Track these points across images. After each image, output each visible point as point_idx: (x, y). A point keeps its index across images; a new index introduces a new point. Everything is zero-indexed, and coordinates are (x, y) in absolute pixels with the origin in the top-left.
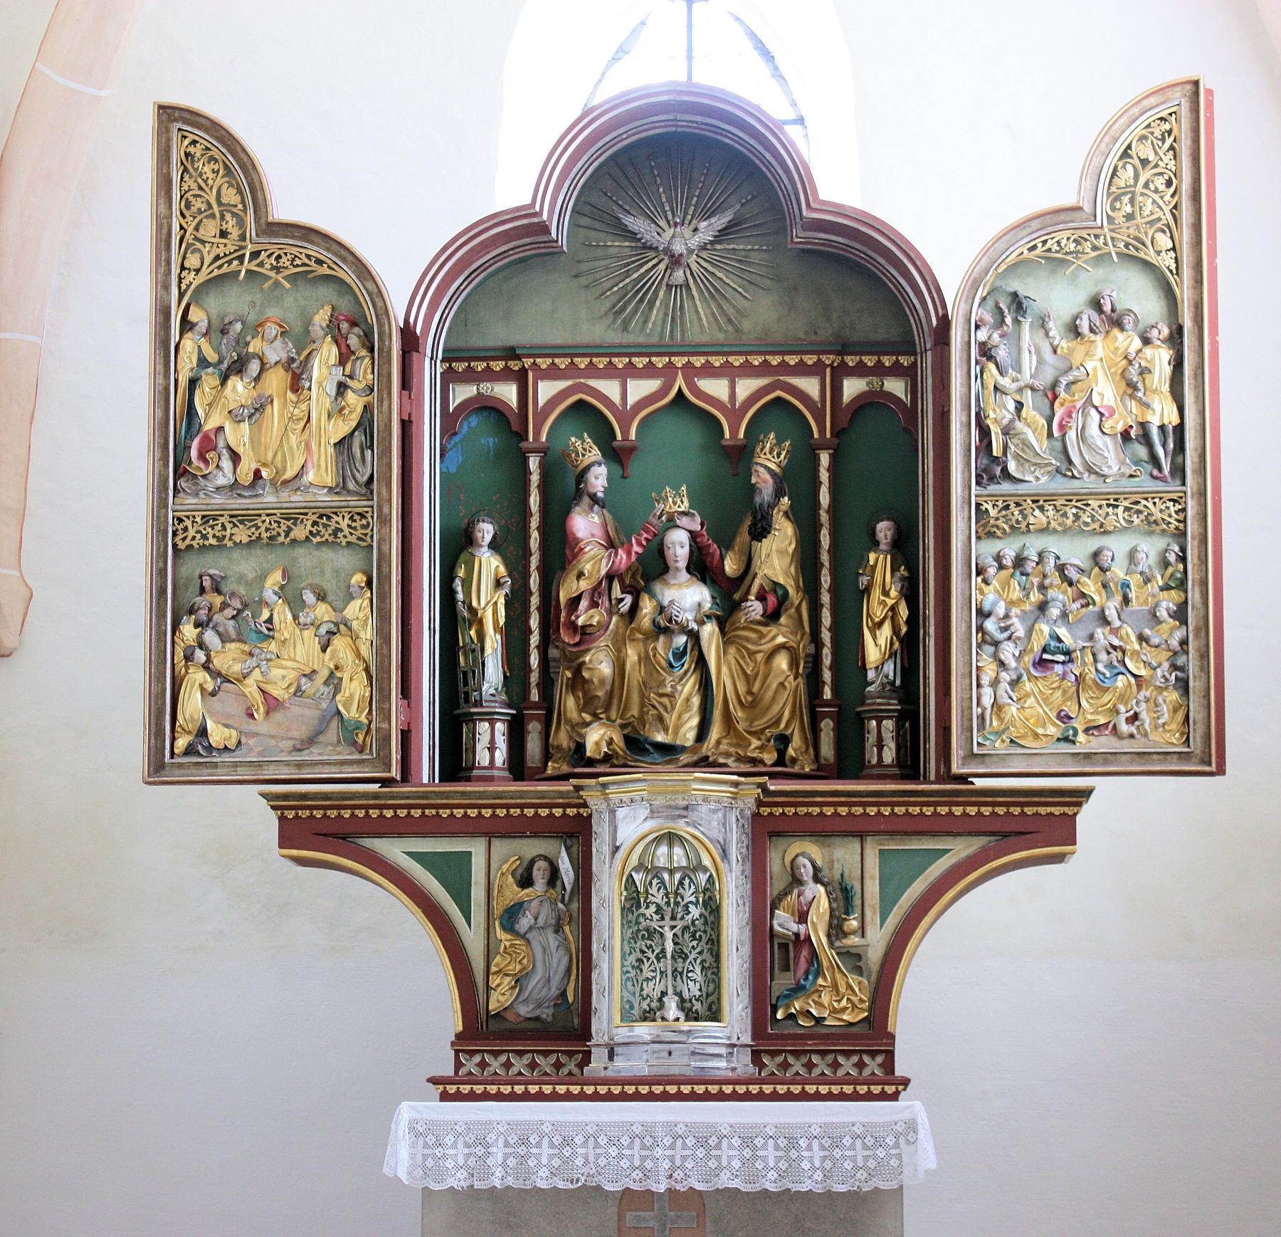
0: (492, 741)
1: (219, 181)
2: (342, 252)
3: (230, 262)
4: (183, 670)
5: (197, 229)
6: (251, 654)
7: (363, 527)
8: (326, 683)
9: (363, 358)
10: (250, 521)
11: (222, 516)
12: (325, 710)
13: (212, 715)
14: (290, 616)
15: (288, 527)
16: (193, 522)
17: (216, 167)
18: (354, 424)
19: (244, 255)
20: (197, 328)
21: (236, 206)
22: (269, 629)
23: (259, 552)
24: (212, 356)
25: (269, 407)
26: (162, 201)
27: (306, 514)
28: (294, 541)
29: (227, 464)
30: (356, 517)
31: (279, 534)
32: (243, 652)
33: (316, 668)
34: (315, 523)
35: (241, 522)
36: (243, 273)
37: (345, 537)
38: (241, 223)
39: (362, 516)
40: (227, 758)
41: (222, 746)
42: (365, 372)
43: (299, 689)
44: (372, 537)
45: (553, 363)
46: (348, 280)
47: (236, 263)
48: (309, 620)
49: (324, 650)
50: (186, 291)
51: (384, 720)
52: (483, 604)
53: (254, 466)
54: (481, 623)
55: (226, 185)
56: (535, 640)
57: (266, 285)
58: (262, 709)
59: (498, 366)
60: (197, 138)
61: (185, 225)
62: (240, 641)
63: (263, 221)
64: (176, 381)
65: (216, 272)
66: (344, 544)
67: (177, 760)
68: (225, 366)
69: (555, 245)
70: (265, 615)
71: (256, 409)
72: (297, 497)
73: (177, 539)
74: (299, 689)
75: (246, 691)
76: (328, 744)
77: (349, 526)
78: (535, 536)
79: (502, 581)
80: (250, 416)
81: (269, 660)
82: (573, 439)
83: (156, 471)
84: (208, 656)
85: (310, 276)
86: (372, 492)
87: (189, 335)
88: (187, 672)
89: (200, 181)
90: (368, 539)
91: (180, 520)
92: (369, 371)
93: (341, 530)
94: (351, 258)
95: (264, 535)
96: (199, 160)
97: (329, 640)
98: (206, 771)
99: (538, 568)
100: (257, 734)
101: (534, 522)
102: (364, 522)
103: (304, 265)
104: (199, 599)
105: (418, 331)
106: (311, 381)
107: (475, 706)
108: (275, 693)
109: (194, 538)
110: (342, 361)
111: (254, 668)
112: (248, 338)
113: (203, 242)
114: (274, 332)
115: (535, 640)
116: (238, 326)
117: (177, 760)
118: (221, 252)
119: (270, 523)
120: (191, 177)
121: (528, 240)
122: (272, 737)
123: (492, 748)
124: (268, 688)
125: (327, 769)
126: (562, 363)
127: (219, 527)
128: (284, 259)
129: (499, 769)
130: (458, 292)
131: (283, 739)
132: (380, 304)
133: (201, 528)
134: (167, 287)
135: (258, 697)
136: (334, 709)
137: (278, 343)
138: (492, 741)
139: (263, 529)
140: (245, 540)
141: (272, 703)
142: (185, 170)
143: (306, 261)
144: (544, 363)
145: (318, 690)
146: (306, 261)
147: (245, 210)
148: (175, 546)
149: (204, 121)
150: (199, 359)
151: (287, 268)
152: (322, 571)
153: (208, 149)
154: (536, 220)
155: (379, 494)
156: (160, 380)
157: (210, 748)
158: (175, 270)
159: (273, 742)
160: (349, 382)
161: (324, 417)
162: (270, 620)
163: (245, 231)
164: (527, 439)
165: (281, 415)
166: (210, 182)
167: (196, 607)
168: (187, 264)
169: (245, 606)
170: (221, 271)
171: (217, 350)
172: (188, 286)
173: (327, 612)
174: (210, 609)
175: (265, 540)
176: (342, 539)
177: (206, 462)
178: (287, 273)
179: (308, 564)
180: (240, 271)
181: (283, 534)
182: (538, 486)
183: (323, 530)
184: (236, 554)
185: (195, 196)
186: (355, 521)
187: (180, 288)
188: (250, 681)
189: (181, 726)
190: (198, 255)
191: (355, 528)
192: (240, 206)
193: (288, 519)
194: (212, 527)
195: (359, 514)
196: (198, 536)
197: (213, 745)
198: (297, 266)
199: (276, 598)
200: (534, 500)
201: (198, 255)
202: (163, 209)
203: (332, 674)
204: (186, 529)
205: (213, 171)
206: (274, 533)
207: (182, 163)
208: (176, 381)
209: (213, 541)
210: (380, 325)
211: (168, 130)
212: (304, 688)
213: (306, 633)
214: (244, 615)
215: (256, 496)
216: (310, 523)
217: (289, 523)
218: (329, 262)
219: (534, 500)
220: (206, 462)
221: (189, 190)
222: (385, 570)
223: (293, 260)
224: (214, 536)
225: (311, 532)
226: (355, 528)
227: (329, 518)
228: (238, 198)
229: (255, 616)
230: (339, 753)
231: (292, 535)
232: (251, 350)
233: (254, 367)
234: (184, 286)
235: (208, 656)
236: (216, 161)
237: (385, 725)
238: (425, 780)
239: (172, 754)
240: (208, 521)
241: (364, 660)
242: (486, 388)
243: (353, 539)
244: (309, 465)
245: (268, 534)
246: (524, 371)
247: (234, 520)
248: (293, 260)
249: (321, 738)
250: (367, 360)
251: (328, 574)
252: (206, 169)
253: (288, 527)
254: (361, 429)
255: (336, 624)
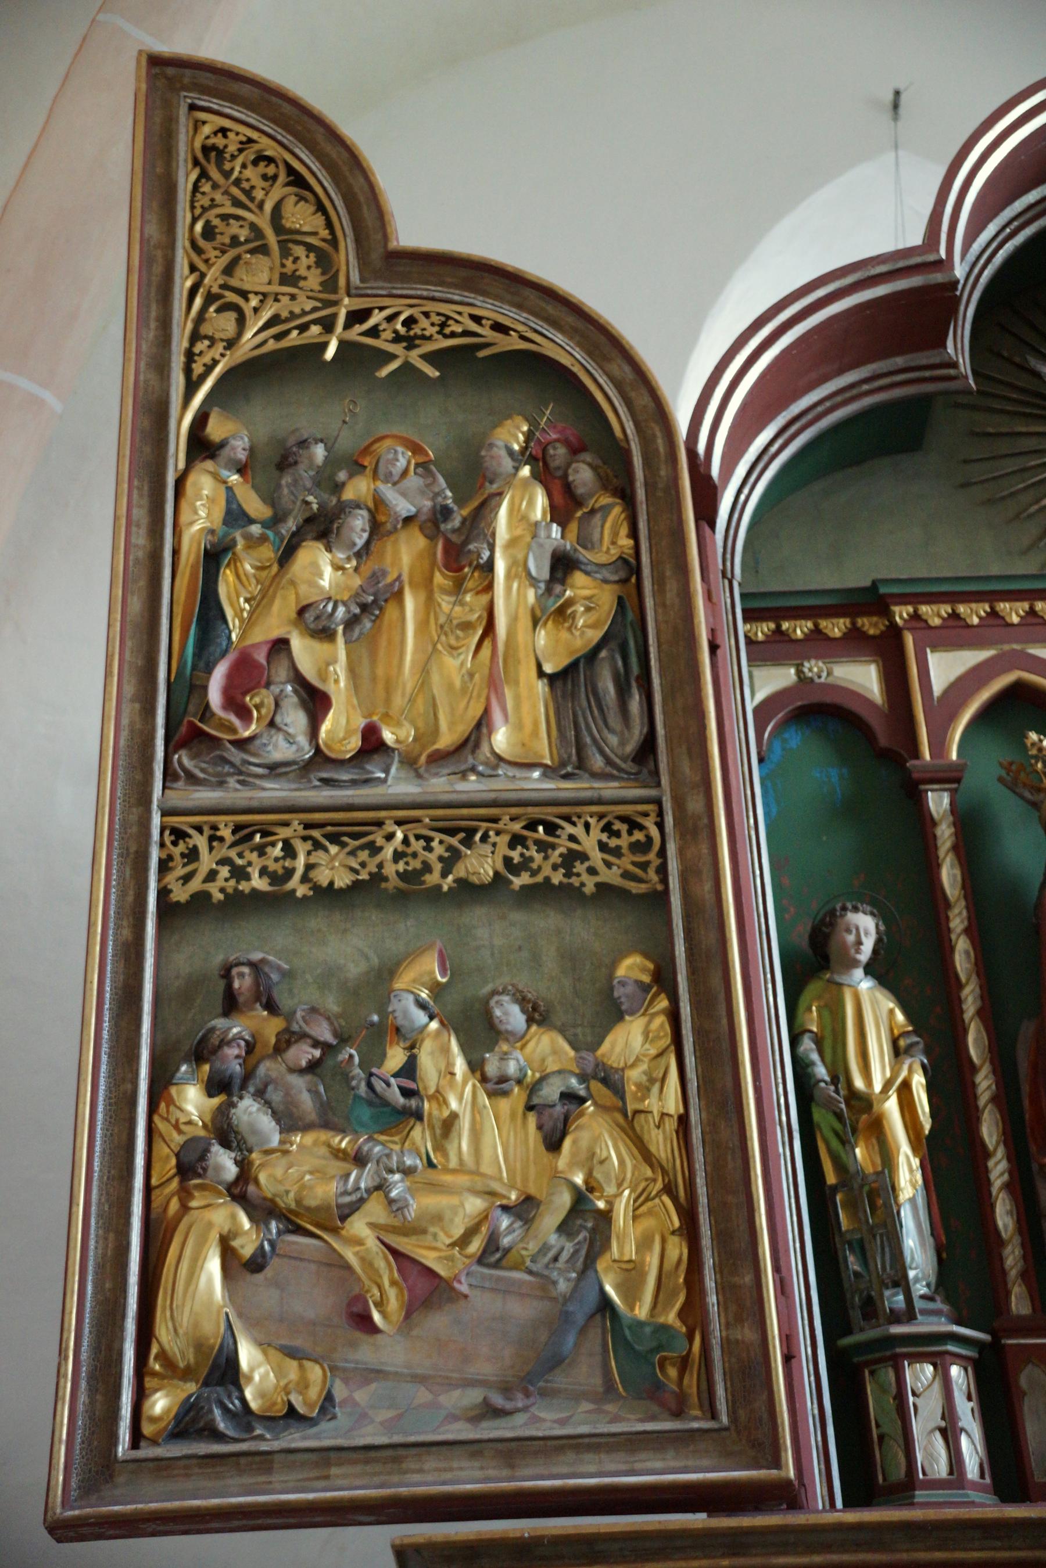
0: (949, 1412)
1: (278, 192)
2: (551, 309)
3: (303, 328)
4: (174, 1205)
5: (229, 270)
6: (360, 1160)
7: (638, 848)
8: (564, 1228)
9: (606, 509)
10: (355, 836)
11: (286, 824)
12: (567, 1299)
13: (254, 1324)
14: (460, 1065)
15: (450, 848)
16: (212, 839)
17: (271, 170)
18: (595, 636)
19: (334, 316)
20: (225, 452)
21: (315, 234)
22: (406, 1093)
23: (375, 916)
24: (254, 505)
25: (391, 611)
26: (153, 218)
27: (495, 820)
28: (463, 884)
29: (295, 719)
30: (617, 826)
31: (427, 868)
32: (338, 1154)
33: (532, 1191)
34: (516, 841)
35: (334, 838)
36: (330, 353)
37: (592, 871)
38: (324, 261)
39: (634, 826)
40: (295, 1439)
41: (281, 1410)
42: (615, 534)
43: (492, 1243)
44: (663, 871)
45: (955, 615)
46: (565, 360)
47: (315, 329)
48: (512, 1068)
49: (553, 1145)
50: (203, 378)
51: (739, 1319)
52: (878, 1087)
53: (361, 722)
54: (877, 1127)
55: (293, 199)
56: (998, 1169)
57: (384, 372)
58: (393, 1303)
59: (836, 628)
60: (227, 123)
61: (202, 266)
62: (326, 1125)
63: (376, 256)
64: (176, 552)
65: (272, 345)
66: (589, 888)
67: (146, 1452)
68: (291, 525)
69: (952, 372)
70: (395, 1058)
71: (364, 607)
72: (472, 786)
73: (170, 878)
74: (492, 1243)
75: (350, 1255)
76: (577, 1397)
77: (603, 847)
78: (962, 946)
79: (902, 1043)
80: (351, 623)
81: (408, 1172)
82: (1033, 736)
83: (125, 721)
84: (244, 1165)
85: (481, 354)
86: (656, 773)
87: (209, 464)
88: (185, 1208)
89: (235, 191)
90: (652, 875)
91: (179, 835)
92: (624, 530)
93: (584, 857)
94: (570, 319)
95: (390, 870)
96: (233, 157)
97: (566, 1120)
98: (235, 1481)
99: (980, 1013)
100: (373, 1374)
101: (957, 921)
102: (639, 836)
103: (466, 333)
104: (220, 1023)
105: (715, 471)
106: (492, 548)
107: (895, 1317)
108: (429, 1259)
109: (212, 876)
110: (559, 514)
111: (369, 1191)
112: (342, 476)
113: (244, 294)
114: (402, 463)
115: (998, 1169)
116: (319, 452)
117: (146, 1452)
118: (283, 307)
119: (406, 841)
120: (215, 186)
121: (900, 361)
122: (420, 1379)
123: (950, 1433)
124: (404, 1244)
125: (590, 1463)
126: (973, 613)
127: (277, 851)
128: (424, 323)
129: (974, 1486)
130: (766, 458)
131: (451, 1384)
132: (643, 400)
133: (233, 854)
134: (161, 366)
135: (385, 1268)
136: (592, 1300)
137: (414, 481)
138: (949, 1412)
139: (388, 852)
140: (343, 880)
141: (422, 1285)
142: (204, 175)
143: (473, 327)
144: (934, 614)
145: (545, 1248)
146: (473, 327)
147: (334, 242)
148: (163, 893)
149: (245, 89)
150: (229, 512)
151: (429, 338)
152: (536, 958)
153: (250, 141)
154: (938, 277)
155: (673, 773)
156: (141, 539)
157: (245, 1416)
158: (180, 343)
159: (423, 1395)
160: (584, 555)
161: (525, 622)
162: (409, 1070)
163: (335, 277)
164: (916, 754)
165: (422, 626)
166: (259, 194)
167: (215, 1040)
168: (206, 329)
169: (343, 1039)
170: (285, 343)
171: (270, 498)
172: (209, 369)
173: (555, 1052)
174: (250, 1047)
175: (394, 882)
176: (585, 877)
177: (244, 714)
178: (428, 347)
179: (498, 942)
180: (324, 346)
181: (438, 867)
182: (955, 848)
183: (538, 857)
184: (316, 921)
185: (225, 217)
186: (617, 834)
187: (188, 371)
188: (358, 1226)
189: (163, 1356)
190: (232, 316)
191: (617, 852)
192: (325, 233)
193: (451, 832)
194: (261, 850)
195: (623, 819)
196: (224, 872)
197: (254, 1405)
198: (453, 335)
199: (421, 1017)
200: (949, 875)
201: (232, 316)
202: (153, 230)
203: (580, 1200)
204: (192, 855)
205: (265, 177)
206: (416, 864)
207: (196, 163)
208: (176, 552)
209: (259, 883)
210: (646, 442)
211: (168, 106)
212: (506, 1241)
213: (504, 1104)
214: (343, 1056)
215: (367, 781)
216: (505, 838)
217: (454, 841)
218: (520, 328)
219: (949, 875)
220: (244, 714)
221: (213, 204)
222: (709, 939)
223: (443, 325)
224: (263, 872)
225: (507, 861)
226: (617, 852)
227: (551, 829)
228: (319, 220)
229: (373, 1057)
230: (616, 1419)
231: (460, 871)
232: (348, 495)
233: (358, 525)
234: (198, 369)
235: (244, 1165)
236: (270, 160)
237: (747, 1334)
238: (820, 1507)
239: (137, 1438)
240: (250, 837)
241: (664, 1172)
242: (813, 667)
243: (611, 876)
244: (497, 715)
245: (401, 867)
246: (894, 633)
247: (316, 834)
248: (443, 325)
249: (560, 1380)
250: (617, 510)
251: (550, 962)
252: (249, 173)
253: (450, 848)
254: (613, 645)
255: (583, 1078)
